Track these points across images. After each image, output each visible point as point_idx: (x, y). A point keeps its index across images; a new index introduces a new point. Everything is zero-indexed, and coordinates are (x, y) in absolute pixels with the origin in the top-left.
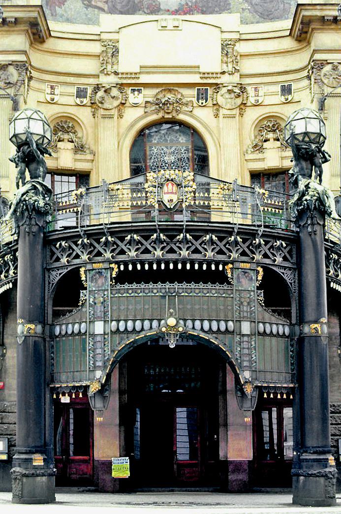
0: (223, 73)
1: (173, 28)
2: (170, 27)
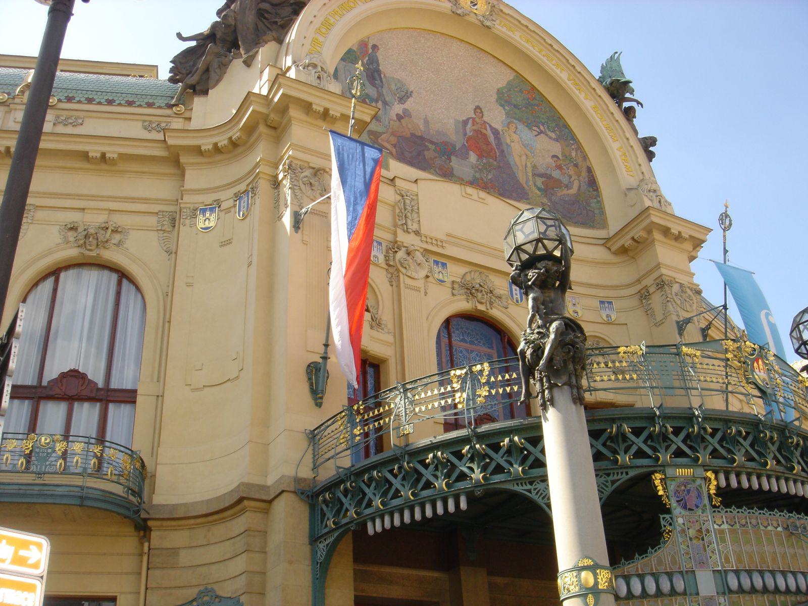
1: (478, 199)
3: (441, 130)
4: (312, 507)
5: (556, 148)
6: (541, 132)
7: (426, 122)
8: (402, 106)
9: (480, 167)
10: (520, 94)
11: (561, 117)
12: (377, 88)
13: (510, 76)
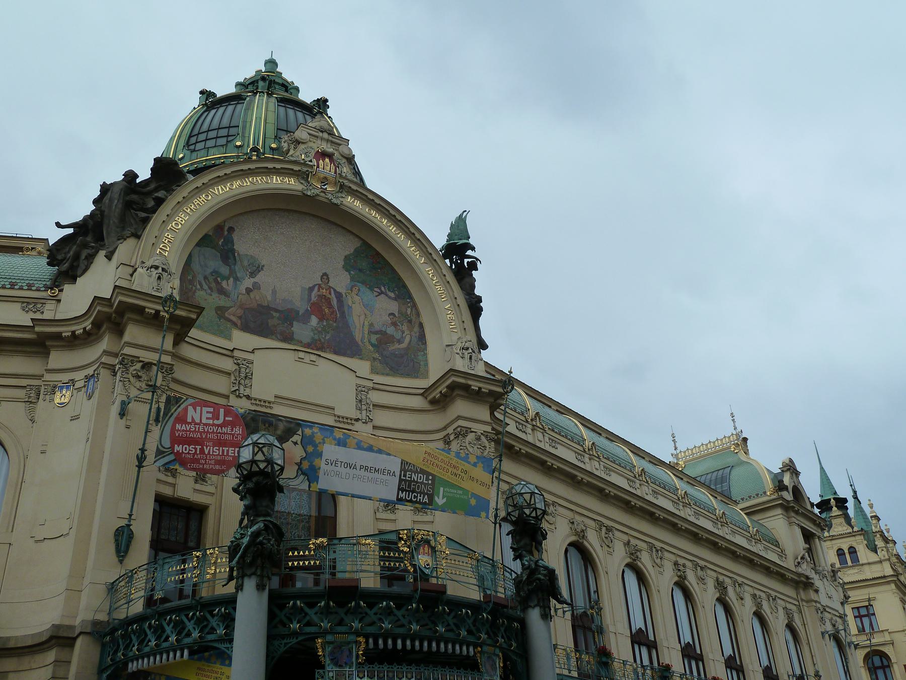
0: (357, 420)
2: (307, 360)
4: (103, 646)
5: (394, 307)
6: (382, 293)
7: (274, 292)
8: (253, 280)
11: (400, 279)
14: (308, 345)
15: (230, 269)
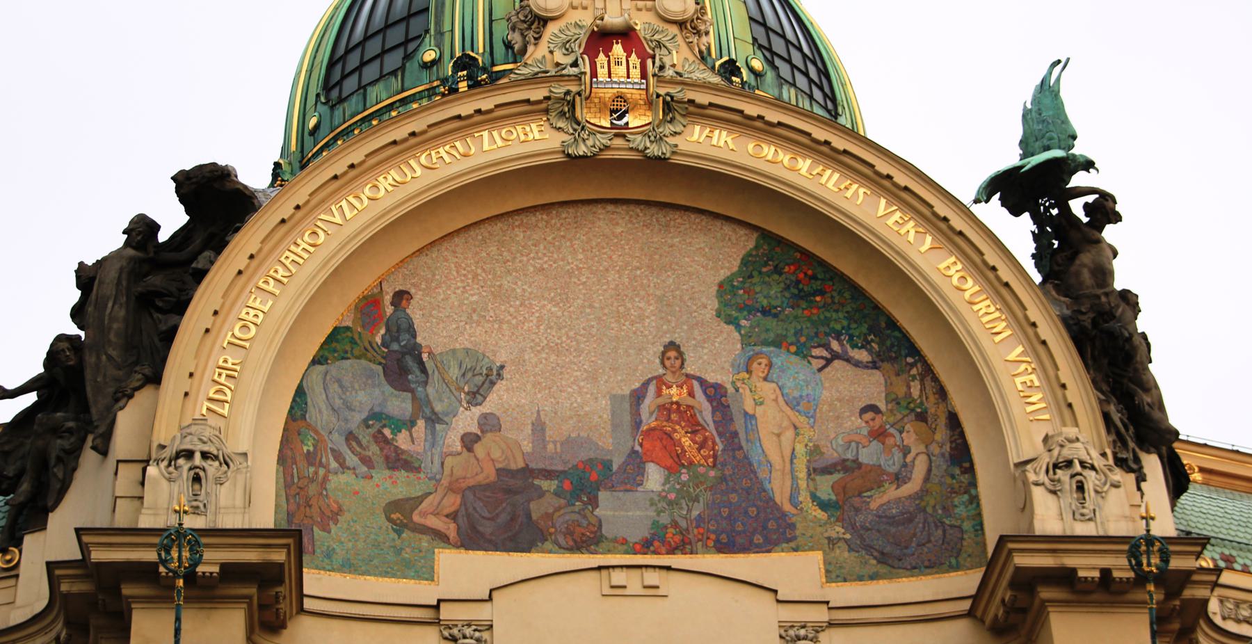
3: (573, 435)
6: (835, 356)
7: (539, 428)
8: (476, 411)
9: (672, 496)
10: (776, 277)
11: (877, 308)
12: (412, 391)
13: (746, 242)
14: (646, 546)
15: (414, 398)
